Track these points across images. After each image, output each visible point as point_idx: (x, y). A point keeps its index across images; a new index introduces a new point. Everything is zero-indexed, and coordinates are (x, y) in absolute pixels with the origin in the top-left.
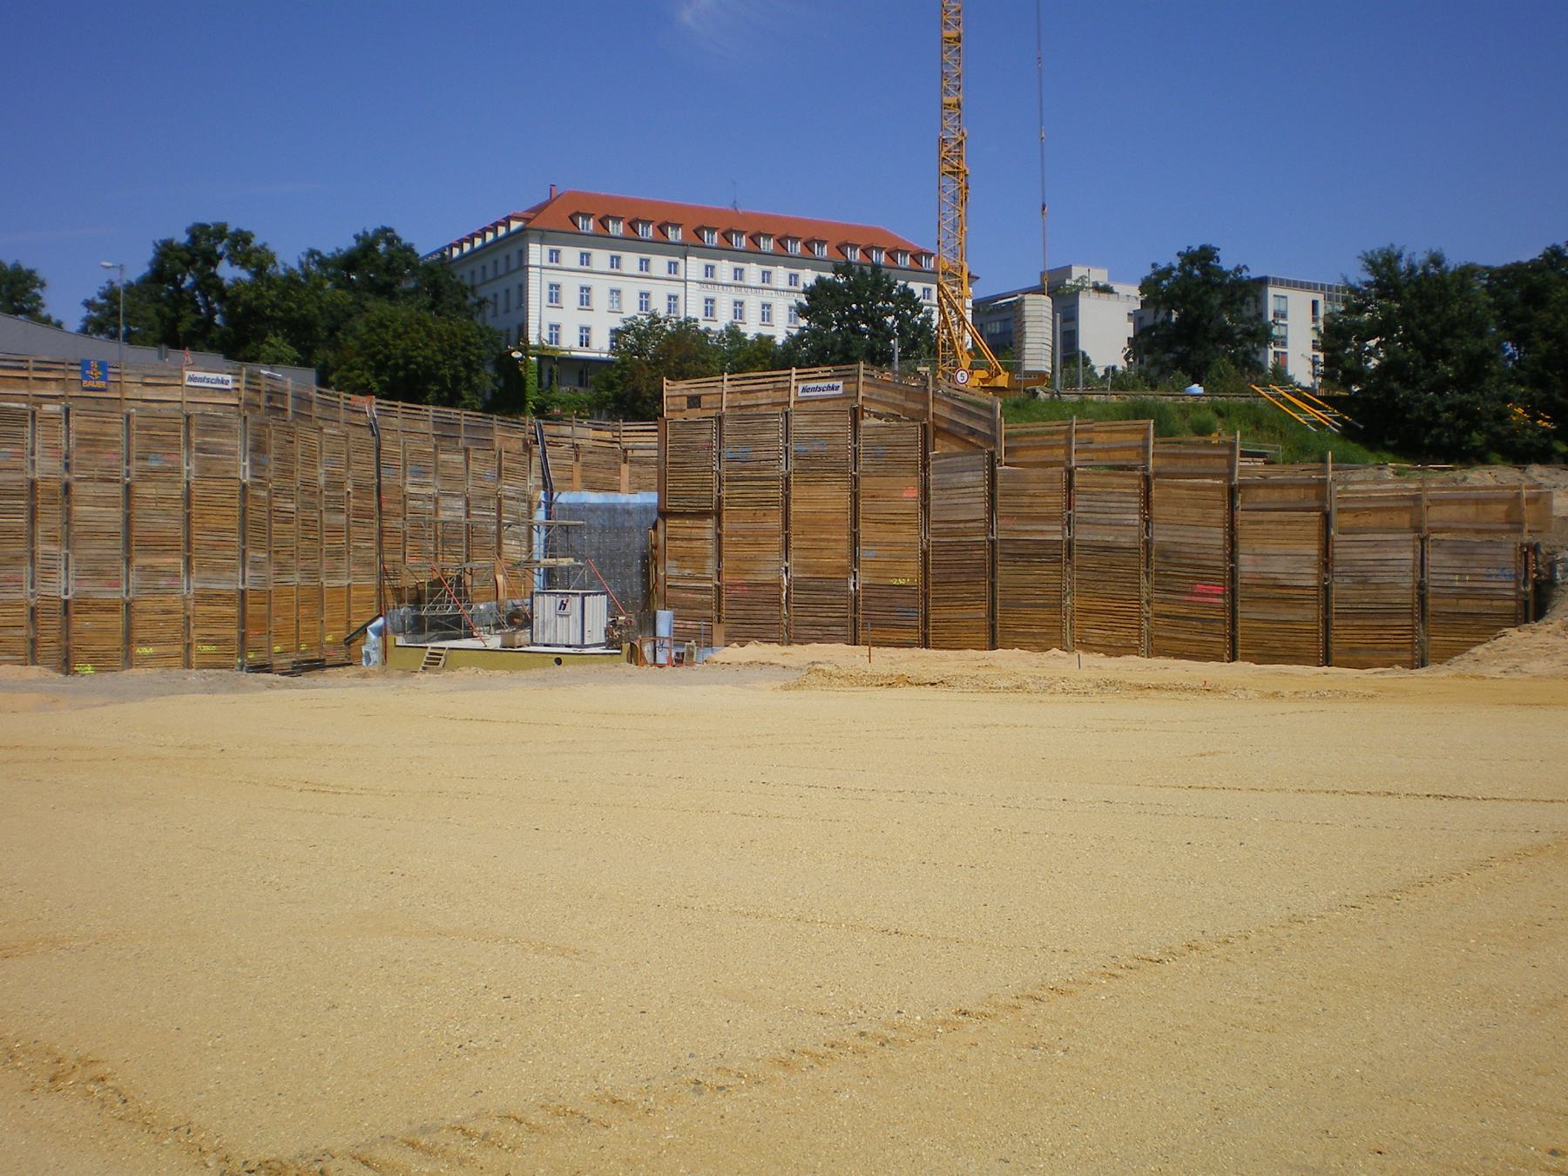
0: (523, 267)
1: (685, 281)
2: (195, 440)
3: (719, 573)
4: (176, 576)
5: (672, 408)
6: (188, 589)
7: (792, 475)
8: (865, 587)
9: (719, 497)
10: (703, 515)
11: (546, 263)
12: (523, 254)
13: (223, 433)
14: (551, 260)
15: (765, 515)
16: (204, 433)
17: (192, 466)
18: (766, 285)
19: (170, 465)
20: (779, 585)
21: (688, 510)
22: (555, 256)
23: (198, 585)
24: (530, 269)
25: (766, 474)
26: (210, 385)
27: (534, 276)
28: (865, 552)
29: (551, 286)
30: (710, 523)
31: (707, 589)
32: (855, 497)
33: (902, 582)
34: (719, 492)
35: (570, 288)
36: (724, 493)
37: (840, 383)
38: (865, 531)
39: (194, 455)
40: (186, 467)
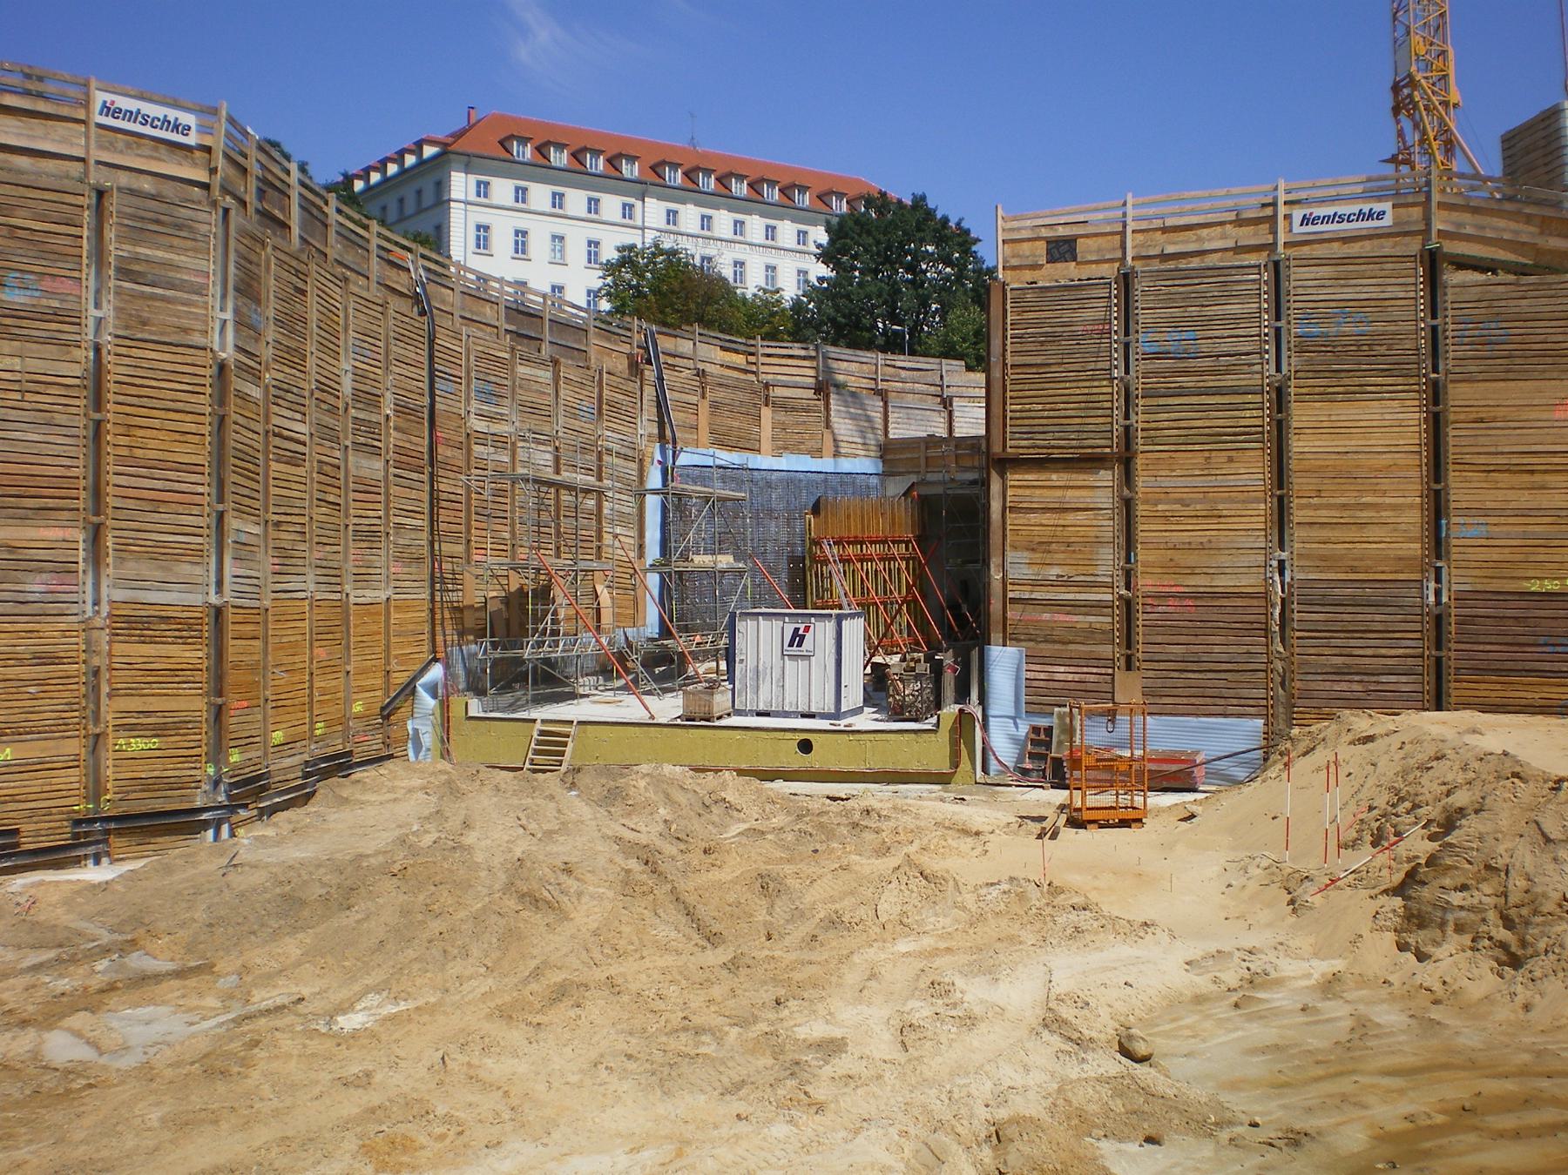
0: (442, 202)
1: (643, 229)
2: (116, 249)
3: (1128, 575)
4: (66, 569)
5: (1014, 262)
6: (96, 603)
7: (1293, 382)
8: (1461, 598)
9: (1127, 428)
10: (1091, 462)
11: (472, 197)
12: (441, 186)
13: (176, 242)
14: (479, 195)
15: (1231, 460)
16: (137, 232)
17: (108, 311)
18: (738, 238)
19: (56, 304)
20: (1266, 596)
21: (1056, 454)
22: (483, 189)
23: (119, 595)
24: (452, 204)
25: (1229, 381)
26: (147, 130)
27: (457, 214)
28: (1459, 529)
29: (479, 227)
30: (1106, 477)
31: (1097, 607)
32: (1436, 425)
33: (1551, 586)
34: (1127, 417)
35: (503, 228)
36: (1138, 420)
37: (1387, 206)
38: (1461, 489)
39: (112, 283)
40: (93, 312)
